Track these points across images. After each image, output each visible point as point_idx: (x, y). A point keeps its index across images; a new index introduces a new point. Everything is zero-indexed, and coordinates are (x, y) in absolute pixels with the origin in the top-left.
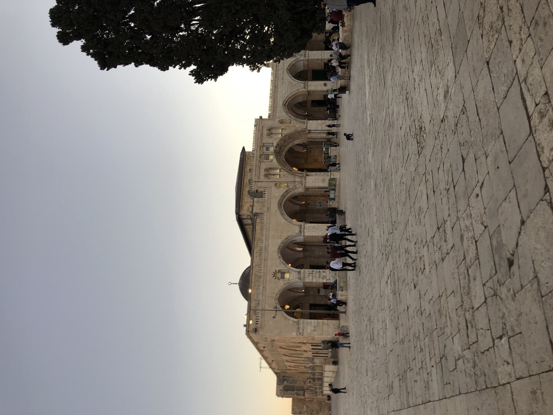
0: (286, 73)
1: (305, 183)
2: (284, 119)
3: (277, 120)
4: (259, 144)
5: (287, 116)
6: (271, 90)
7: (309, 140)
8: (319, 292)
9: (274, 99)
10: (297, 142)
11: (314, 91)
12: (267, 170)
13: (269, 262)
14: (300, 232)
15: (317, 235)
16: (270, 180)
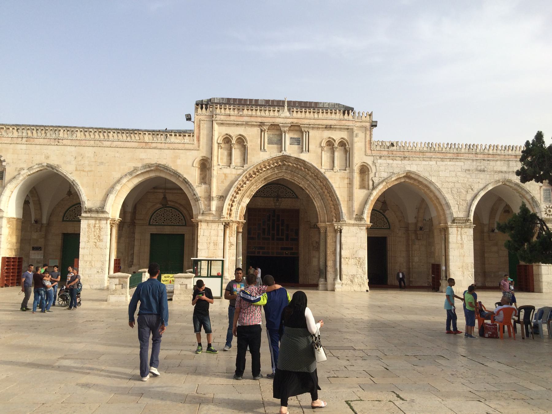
0: (497, 177)
1: (207, 222)
2: (371, 175)
3: (369, 161)
4: (306, 122)
5: (376, 181)
6: (450, 146)
7: (322, 231)
8: (34, 249)
9: (423, 152)
10: (318, 204)
11: (446, 240)
12: (241, 140)
13: (24, 147)
14: (90, 211)
15: (82, 245)
16: (215, 146)
